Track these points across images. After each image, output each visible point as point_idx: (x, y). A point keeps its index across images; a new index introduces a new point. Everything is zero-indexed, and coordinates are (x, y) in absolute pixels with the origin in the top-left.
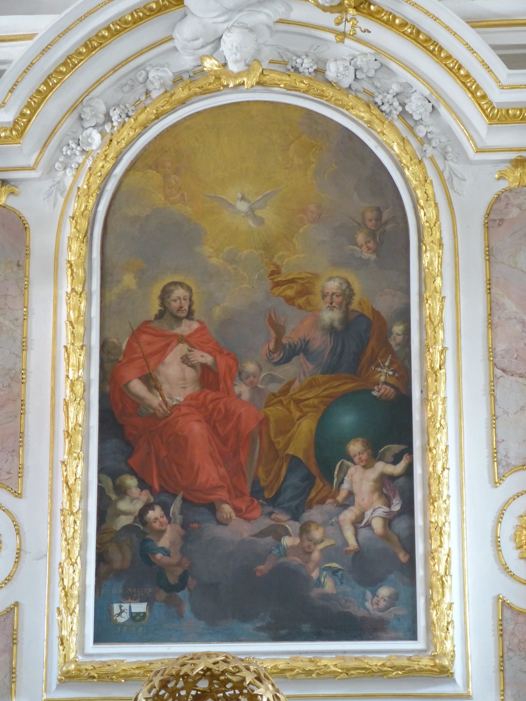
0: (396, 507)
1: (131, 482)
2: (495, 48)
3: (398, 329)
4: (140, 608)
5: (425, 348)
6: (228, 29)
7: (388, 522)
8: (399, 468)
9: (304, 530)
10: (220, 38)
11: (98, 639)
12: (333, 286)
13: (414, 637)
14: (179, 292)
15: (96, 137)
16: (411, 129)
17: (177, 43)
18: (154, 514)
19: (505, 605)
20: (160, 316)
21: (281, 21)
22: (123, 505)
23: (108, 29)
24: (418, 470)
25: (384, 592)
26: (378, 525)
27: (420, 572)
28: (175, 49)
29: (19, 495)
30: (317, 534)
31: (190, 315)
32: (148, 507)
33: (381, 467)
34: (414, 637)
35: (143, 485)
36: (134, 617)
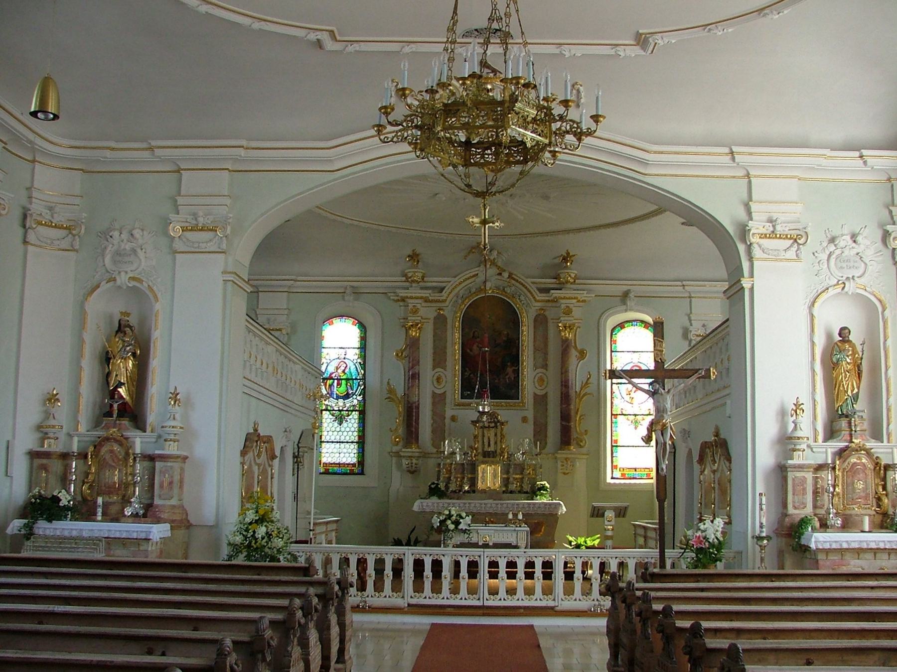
0: (516, 375)
1: (467, 369)
3: (517, 341)
4: (469, 393)
5: (522, 345)
7: (514, 378)
8: (517, 368)
9: (499, 380)
11: (461, 398)
12: (506, 333)
13: (518, 399)
14: (476, 333)
15: (460, 301)
16: (521, 302)
18: (472, 375)
19: (535, 394)
20: (473, 337)
22: (466, 374)
24: (520, 368)
25: (513, 391)
26: (513, 378)
27: (520, 388)
29: (446, 370)
30: (501, 380)
31: (478, 337)
32: (470, 374)
33: (514, 368)
34: (518, 399)
35: (470, 370)
36: (468, 394)
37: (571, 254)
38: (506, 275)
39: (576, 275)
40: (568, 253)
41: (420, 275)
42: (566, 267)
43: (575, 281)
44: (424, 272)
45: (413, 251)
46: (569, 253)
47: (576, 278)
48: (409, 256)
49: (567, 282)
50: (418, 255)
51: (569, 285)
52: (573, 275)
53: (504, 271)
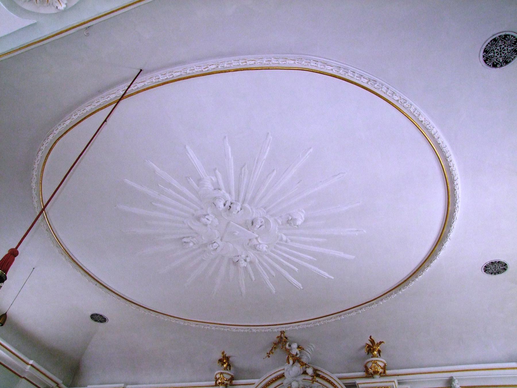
2: (343, 384)
6: (293, 381)
10: (291, 384)
17: (284, 384)
21: (304, 379)
23: (270, 382)
28: (283, 385)
37: (376, 343)
38: (310, 371)
39: (385, 365)
40: (372, 341)
41: (229, 377)
42: (374, 356)
43: (384, 372)
44: (232, 374)
45: (223, 353)
46: (373, 341)
47: (384, 368)
48: (220, 361)
49: (376, 372)
50: (227, 358)
51: (377, 376)
52: (382, 365)
53: (309, 367)
